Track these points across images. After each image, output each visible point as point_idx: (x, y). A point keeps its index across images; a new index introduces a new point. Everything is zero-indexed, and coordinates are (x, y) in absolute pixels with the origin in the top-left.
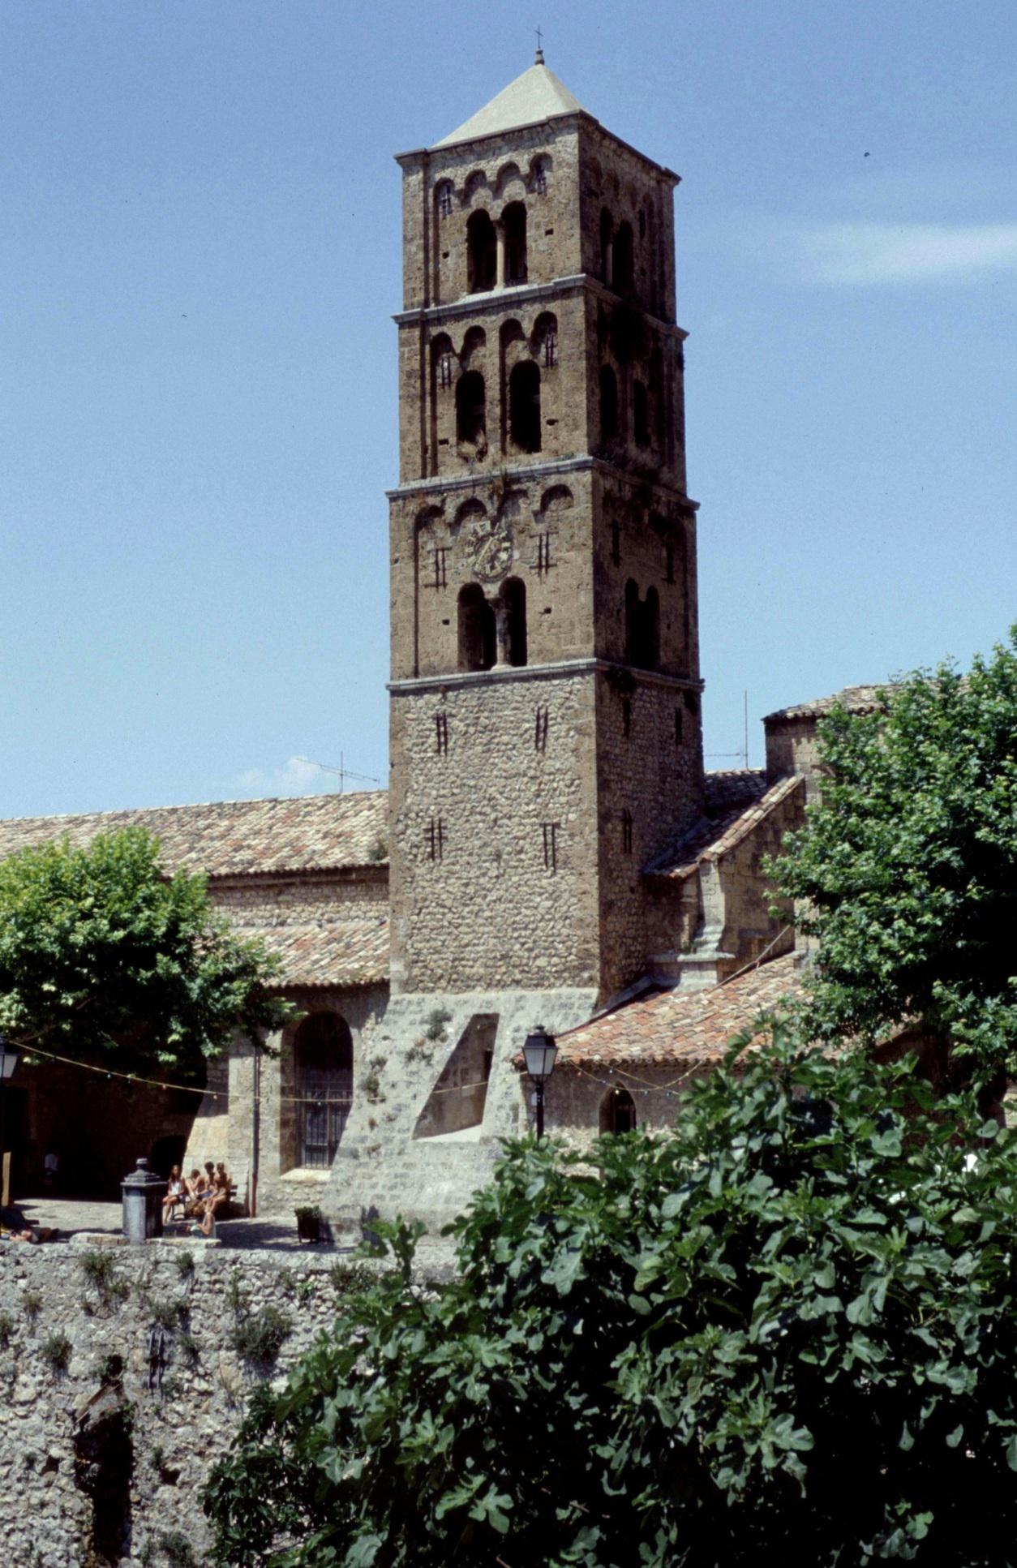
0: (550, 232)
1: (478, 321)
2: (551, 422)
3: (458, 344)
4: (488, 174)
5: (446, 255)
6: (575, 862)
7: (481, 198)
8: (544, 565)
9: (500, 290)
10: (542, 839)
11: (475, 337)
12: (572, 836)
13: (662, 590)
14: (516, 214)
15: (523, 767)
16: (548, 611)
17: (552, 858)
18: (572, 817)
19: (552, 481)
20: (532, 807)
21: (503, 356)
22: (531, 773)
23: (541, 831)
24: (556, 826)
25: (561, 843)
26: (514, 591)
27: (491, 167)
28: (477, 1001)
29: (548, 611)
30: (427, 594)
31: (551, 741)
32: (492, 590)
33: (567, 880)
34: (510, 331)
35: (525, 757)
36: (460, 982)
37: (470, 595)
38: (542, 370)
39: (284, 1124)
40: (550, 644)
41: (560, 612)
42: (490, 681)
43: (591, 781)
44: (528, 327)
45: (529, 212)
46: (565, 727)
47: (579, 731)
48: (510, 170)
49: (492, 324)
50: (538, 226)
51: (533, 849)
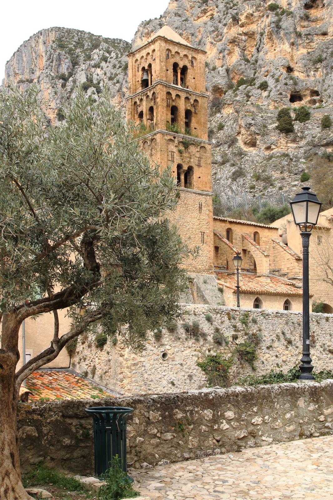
0: (194, 78)
1: (180, 93)
2: (195, 128)
4: (181, 54)
5: (167, 70)
6: (208, 243)
7: (177, 59)
8: (199, 166)
10: (200, 236)
11: (178, 96)
12: (207, 236)
15: (196, 216)
16: (200, 178)
17: (203, 241)
18: (208, 232)
19: (202, 145)
20: (198, 227)
22: (198, 218)
23: (200, 233)
24: (204, 232)
25: (205, 237)
26: (190, 169)
27: (183, 52)
29: (200, 178)
31: (202, 211)
32: (185, 167)
35: (196, 214)
37: (179, 167)
38: (193, 114)
40: (200, 186)
41: (204, 179)
42: (187, 191)
45: (189, 71)
46: (206, 209)
47: (209, 210)
50: (192, 75)
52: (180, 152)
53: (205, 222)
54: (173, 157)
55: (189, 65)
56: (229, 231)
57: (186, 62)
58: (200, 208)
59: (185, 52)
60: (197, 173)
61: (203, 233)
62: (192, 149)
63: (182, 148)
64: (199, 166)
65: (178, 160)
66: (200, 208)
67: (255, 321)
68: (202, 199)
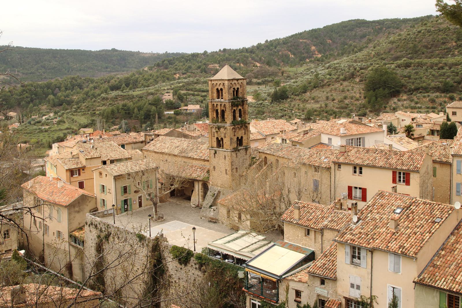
1: (217, 103)
3: (215, 106)
8: (225, 137)
9: (220, 100)
13: (243, 136)
14: (221, 89)
17: (226, 173)
21: (220, 108)
25: (227, 171)
28: (219, 188)
30: (213, 137)
33: (228, 176)
34: (221, 105)
35: (223, 160)
36: (218, 186)
39: (202, 196)
43: (230, 165)
44: (223, 106)
48: (220, 84)
49: (219, 104)
51: (225, 172)
52: (217, 132)
53: (227, 165)
54: (214, 134)
55: (222, 88)
56: (277, 160)
57: (221, 87)
58: (225, 158)
59: (220, 82)
60: (225, 140)
61: (226, 170)
62: (222, 130)
63: (217, 130)
64: (225, 137)
65: (216, 136)
66: (225, 158)
67: (110, 228)
68: (226, 154)
